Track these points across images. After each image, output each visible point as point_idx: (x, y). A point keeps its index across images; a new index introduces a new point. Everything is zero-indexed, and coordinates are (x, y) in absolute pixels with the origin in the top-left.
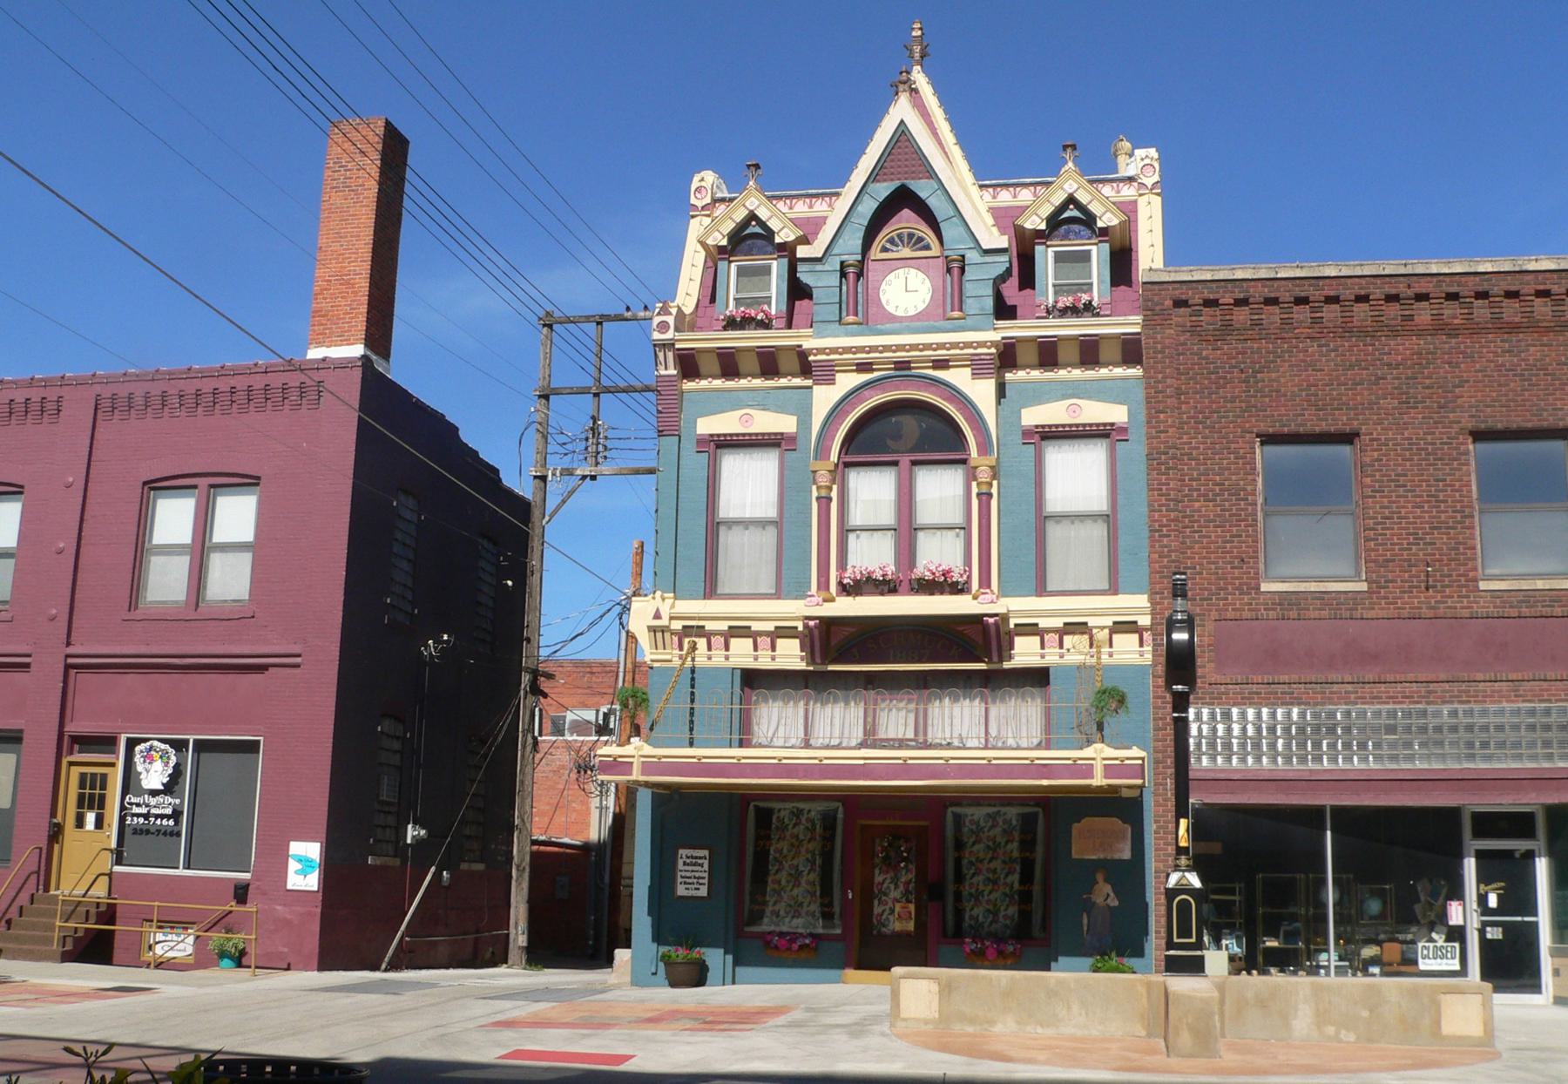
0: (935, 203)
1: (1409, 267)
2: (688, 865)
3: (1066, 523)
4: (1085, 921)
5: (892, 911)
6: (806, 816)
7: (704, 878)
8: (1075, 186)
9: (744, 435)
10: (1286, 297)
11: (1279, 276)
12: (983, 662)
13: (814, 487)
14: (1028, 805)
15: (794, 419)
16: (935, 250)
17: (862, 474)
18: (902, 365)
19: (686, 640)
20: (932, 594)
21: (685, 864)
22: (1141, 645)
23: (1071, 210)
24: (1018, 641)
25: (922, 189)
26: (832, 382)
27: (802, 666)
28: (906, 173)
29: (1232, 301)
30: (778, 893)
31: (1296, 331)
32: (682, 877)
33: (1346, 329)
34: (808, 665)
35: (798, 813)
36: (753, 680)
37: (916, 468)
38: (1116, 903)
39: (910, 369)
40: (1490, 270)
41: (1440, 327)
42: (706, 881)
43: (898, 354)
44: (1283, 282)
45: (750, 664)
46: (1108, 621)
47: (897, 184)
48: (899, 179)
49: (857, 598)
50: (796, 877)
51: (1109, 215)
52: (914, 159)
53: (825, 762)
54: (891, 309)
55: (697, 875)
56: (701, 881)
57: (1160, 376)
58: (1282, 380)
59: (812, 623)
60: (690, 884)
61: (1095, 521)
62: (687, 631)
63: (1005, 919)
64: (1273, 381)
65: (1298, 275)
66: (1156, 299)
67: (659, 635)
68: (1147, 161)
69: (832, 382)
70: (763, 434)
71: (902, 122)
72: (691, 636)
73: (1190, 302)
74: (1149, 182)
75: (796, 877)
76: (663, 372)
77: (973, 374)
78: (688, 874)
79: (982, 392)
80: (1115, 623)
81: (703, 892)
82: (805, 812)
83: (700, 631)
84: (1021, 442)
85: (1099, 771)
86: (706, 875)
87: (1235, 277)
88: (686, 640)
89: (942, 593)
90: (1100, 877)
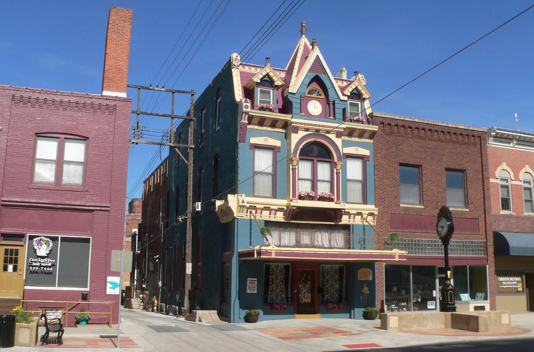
0: (326, 82)
1: (434, 122)
2: (251, 283)
3: (351, 183)
4: (361, 298)
5: (304, 296)
6: (279, 267)
7: (255, 287)
8: (358, 84)
9: (264, 145)
11: (406, 120)
12: (334, 222)
13: (291, 165)
15: (280, 142)
16: (323, 96)
17: (302, 162)
18: (318, 131)
19: (249, 210)
20: (324, 201)
21: (249, 283)
24: (344, 216)
25: (323, 77)
26: (297, 133)
27: (283, 220)
28: (318, 71)
30: (272, 291)
32: (249, 287)
33: (419, 137)
34: (285, 220)
35: (277, 266)
36: (268, 223)
38: (368, 292)
39: (319, 132)
40: (451, 126)
41: (439, 140)
42: (256, 288)
43: (317, 127)
44: (406, 122)
45: (267, 219)
46: (367, 212)
49: (304, 201)
50: (277, 286)
51: (366, 94)
53: (328, 253)
54: (311, 112)
55: (253, 286)
56: (255, 288)
59: (294, 208)
61: (359, 183)
62: (251, 207)
66: (376, 121)
68: (363, 78)
69: (297, 133)
70: (270, 146)
71: (317, 56)
72: (251, 209)
73: (384, 123)
75: (277, 286)
76: (243, 122)
77: (336, 136)
78: (251, 286)
79: (338, 142)
80: (369, 213)
81: (255, 292)
82: (279, 266)
83: (255, 208)
85: (397, 257)
86: (256, 286)
87: (395, 118)
88: (249, 210)
89: (326, 201)
90: (365, 285)
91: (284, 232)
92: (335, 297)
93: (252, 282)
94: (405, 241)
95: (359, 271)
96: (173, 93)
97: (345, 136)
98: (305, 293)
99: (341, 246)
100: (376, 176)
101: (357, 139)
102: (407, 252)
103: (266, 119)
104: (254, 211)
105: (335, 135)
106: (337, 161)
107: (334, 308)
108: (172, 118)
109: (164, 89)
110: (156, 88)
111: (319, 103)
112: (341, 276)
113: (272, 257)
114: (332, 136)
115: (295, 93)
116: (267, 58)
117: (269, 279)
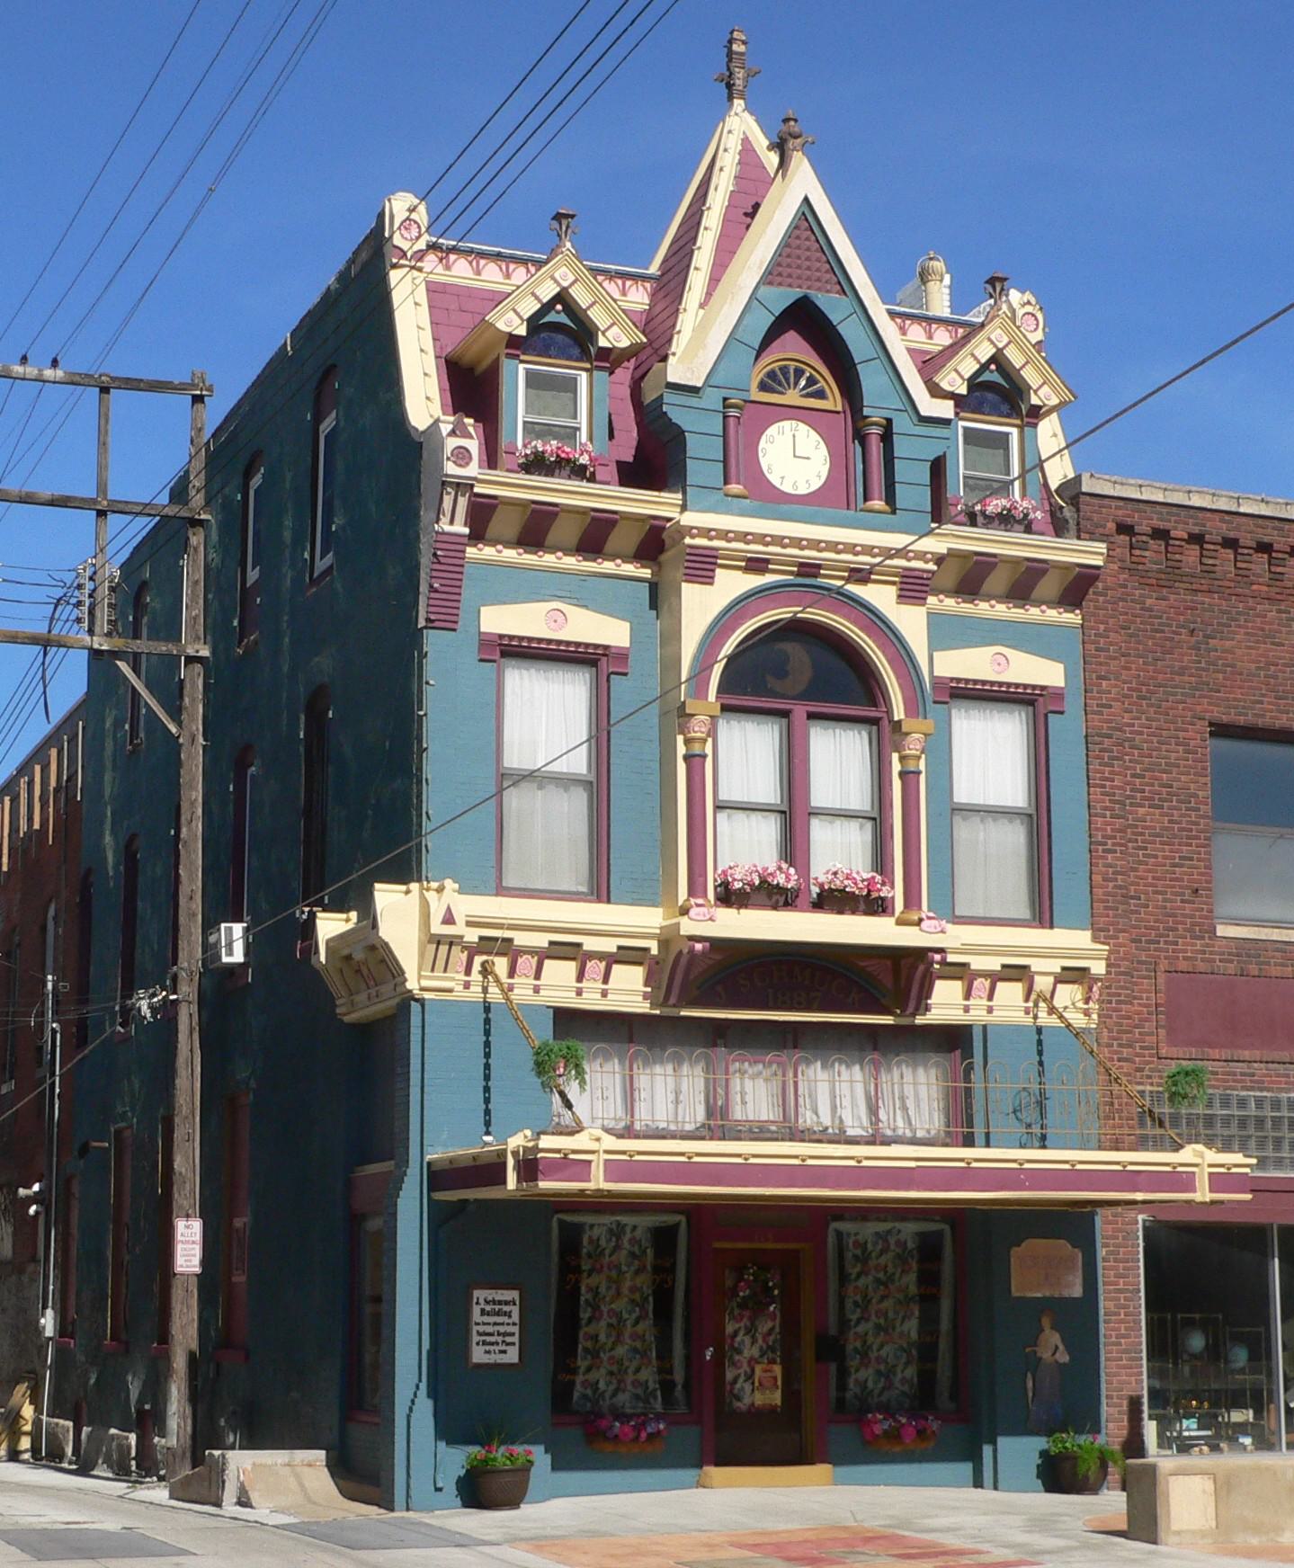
0: (851, 332)
2: (488, 1314)
3: (976, 819)
4: (1030, 1384)
5: (750, 1377)
6: (628, 1236)
7: (513, 1334)
8: (1006, 340)
9: (549, 641)
10: (1144, 527)
11: (1242, 510)
13: (680, 739)
14: (933, 1221)
16: (834, 401)
17: (734, 723)
19: (478, 960)
20: (841, 912)
21: (483, 1312)
23: (992, 372)
25: (832, 306)
26: (708, 579)
27: (643, 1007)
28: (808, 279)
29: (1186, 537)
30: (594, 1354)
31: (1255, 587)
32: (479, 1334)
34: (653, 1006)
35: (617, 1232)
36: (569, 1022)
37: (811, 722)
38: (1063, 1357)
39: (816, 576)
42: (516, 1339)
43: (807, 553)
44: (1244, 519)
45: (569, 1000)
46: (1055, 966)
47: (793, 294)
48: (800, 287)
49: (743, 911)
50: (617, 1328)
52: (818, 260)
53: (866, 1163)
54: (774, 479)
55: (502, 1329)
56: (508, 1339)
57: (1102, 627)
59: (699, 946)
60: (492, 1344)
61: (1011, 821)
62: (486, 945)
63: (903, 1384)
65: (1263, 513)
66: (1096, 517)
67: (444, 949)
68: (1029, 309)
69: (708, 579)
70: (578, 644)
71: (806, 200)
72: (489, 953)
73: (1137, 529)
75: (617, 1328)
76: (447, 528)
77: (899, 596)
78: (489, 1329)
79: (911, 622)
80: (1064, 969)
81: (512, 1356)
82: (628, 1230)
83: (506, 947)
86: (516, 1329)
87: (1190, 503)
89: (853, 912)
90: (1046, 1322)
91: (646, 1063)
92: (904, 1380)
93: (497, 1307)
94: (1242, 1103)
95: (1015, 1251)
96: (105, 390)
97: (942, 592)
98: (752, 1362)
99: (928, 1131)
100: (1096, 786)
101: (1001, 607)
102: (1254, 1161)
103: (556, 514)
104: (501, 965)
105: (892, 591)
106: (902, 716)
107: (894, 1436)
108: (101, 514)
109: (60, 373)
110: (18, 369)
111: (812, 432)
112: (929, 1279)
113: (591, 1186)
114: (881, 596)
115: (699, 384)
116: (558, 217)
117: (576, 1292)
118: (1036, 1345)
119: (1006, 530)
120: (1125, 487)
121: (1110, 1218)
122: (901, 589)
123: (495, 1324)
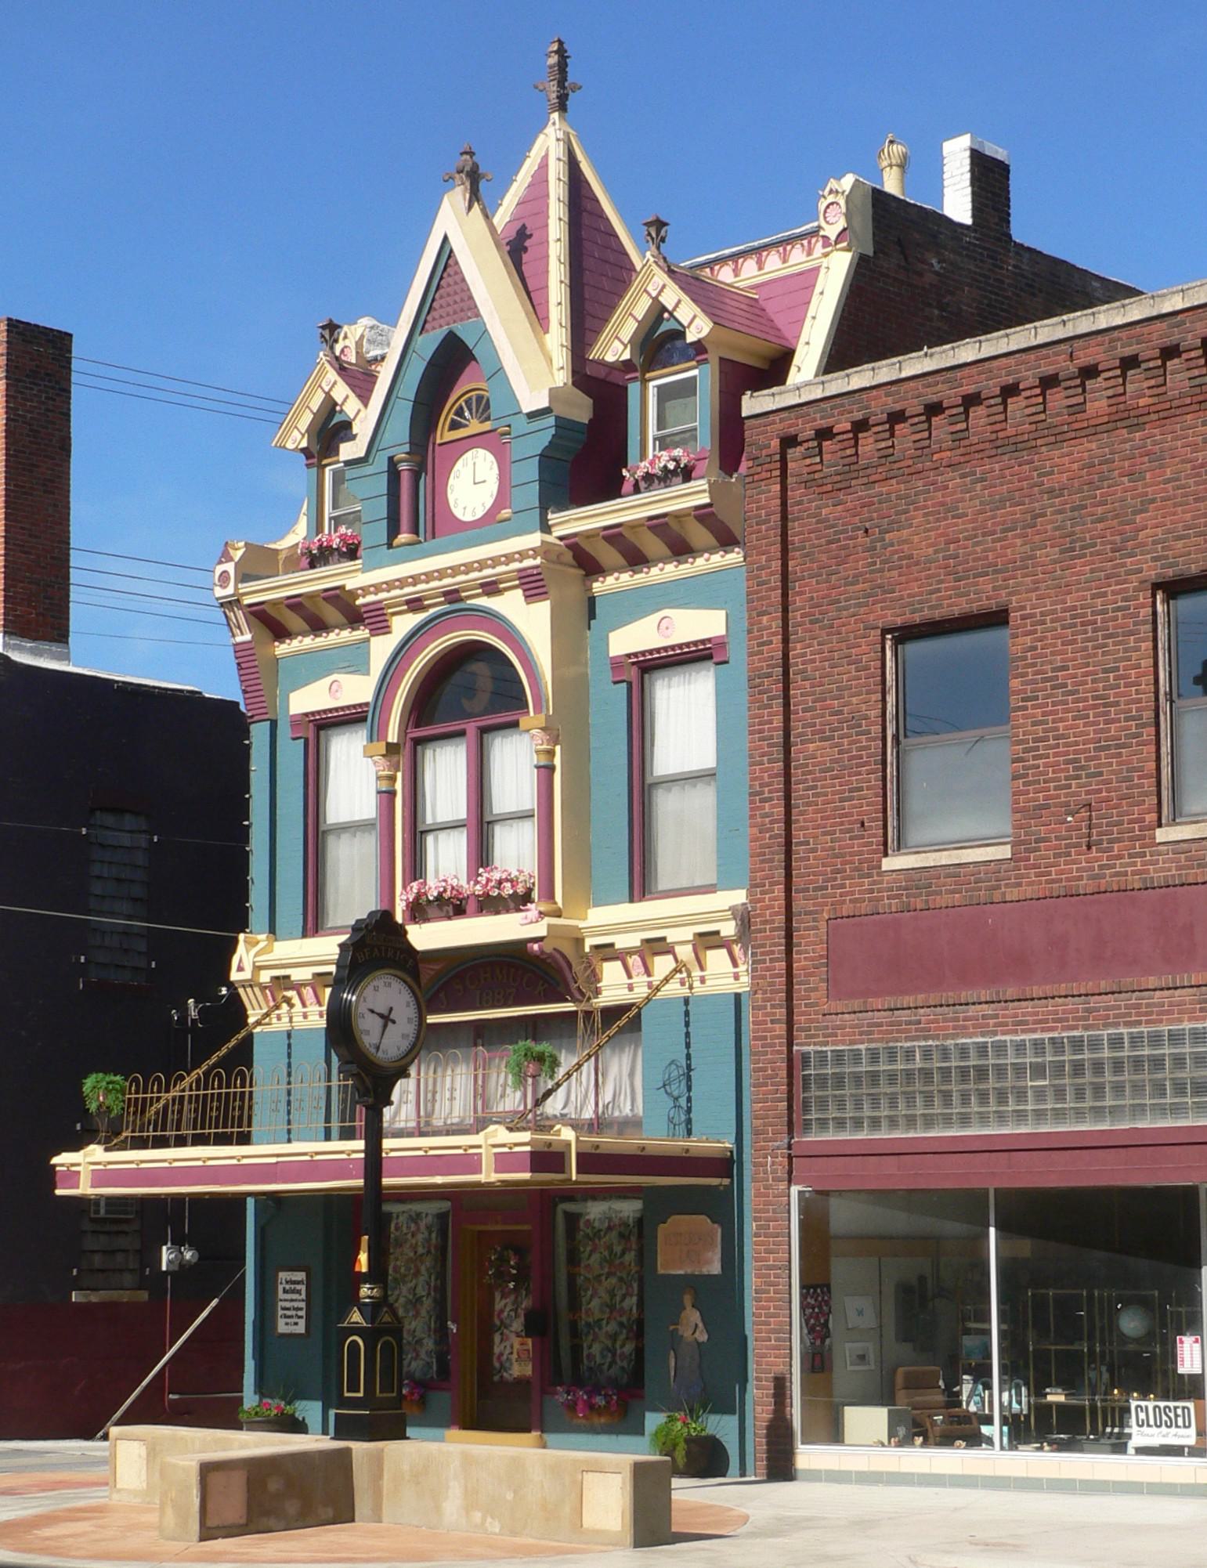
1: (1070, 325)
3: (676, 789)
7: (301, 1309)
11: (904, 375)
20: (498, 913)
22: (735, 964)
31: (935, 457)
33: (1000, 445)
38: (702, 1337)
39: (461, 600)
40: (1180, 306)
41: (1124, 418)
42: (302, 1313)
43: (447, 581)
44: (912, 384)
46: (688, 933)
47: (445, 330)
58: (916, 539)
63: (622, 1361)
64: (906, 542)
74: (832, 232)
84: (611, 679)
85: (487, 1163)
86: (303, 1305)
89: (508, 911)
90: (688, 1300)
94: (909, 1054)
101: (670, 567)
113: (482, 1178)
116: (660, 224)
118: (677, 1324)
119: (666, 487)
120: (783, 396)
121: (762, 1190)
122: (525, 590)
123: (292, 1300)
